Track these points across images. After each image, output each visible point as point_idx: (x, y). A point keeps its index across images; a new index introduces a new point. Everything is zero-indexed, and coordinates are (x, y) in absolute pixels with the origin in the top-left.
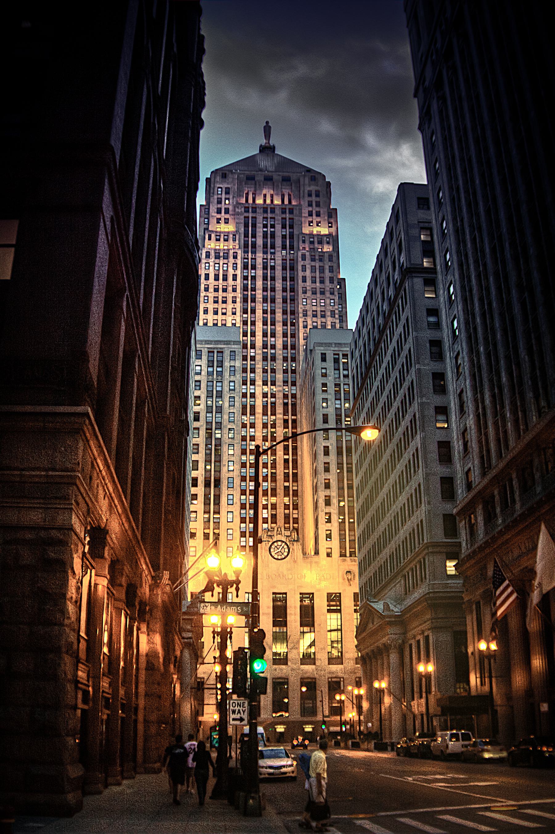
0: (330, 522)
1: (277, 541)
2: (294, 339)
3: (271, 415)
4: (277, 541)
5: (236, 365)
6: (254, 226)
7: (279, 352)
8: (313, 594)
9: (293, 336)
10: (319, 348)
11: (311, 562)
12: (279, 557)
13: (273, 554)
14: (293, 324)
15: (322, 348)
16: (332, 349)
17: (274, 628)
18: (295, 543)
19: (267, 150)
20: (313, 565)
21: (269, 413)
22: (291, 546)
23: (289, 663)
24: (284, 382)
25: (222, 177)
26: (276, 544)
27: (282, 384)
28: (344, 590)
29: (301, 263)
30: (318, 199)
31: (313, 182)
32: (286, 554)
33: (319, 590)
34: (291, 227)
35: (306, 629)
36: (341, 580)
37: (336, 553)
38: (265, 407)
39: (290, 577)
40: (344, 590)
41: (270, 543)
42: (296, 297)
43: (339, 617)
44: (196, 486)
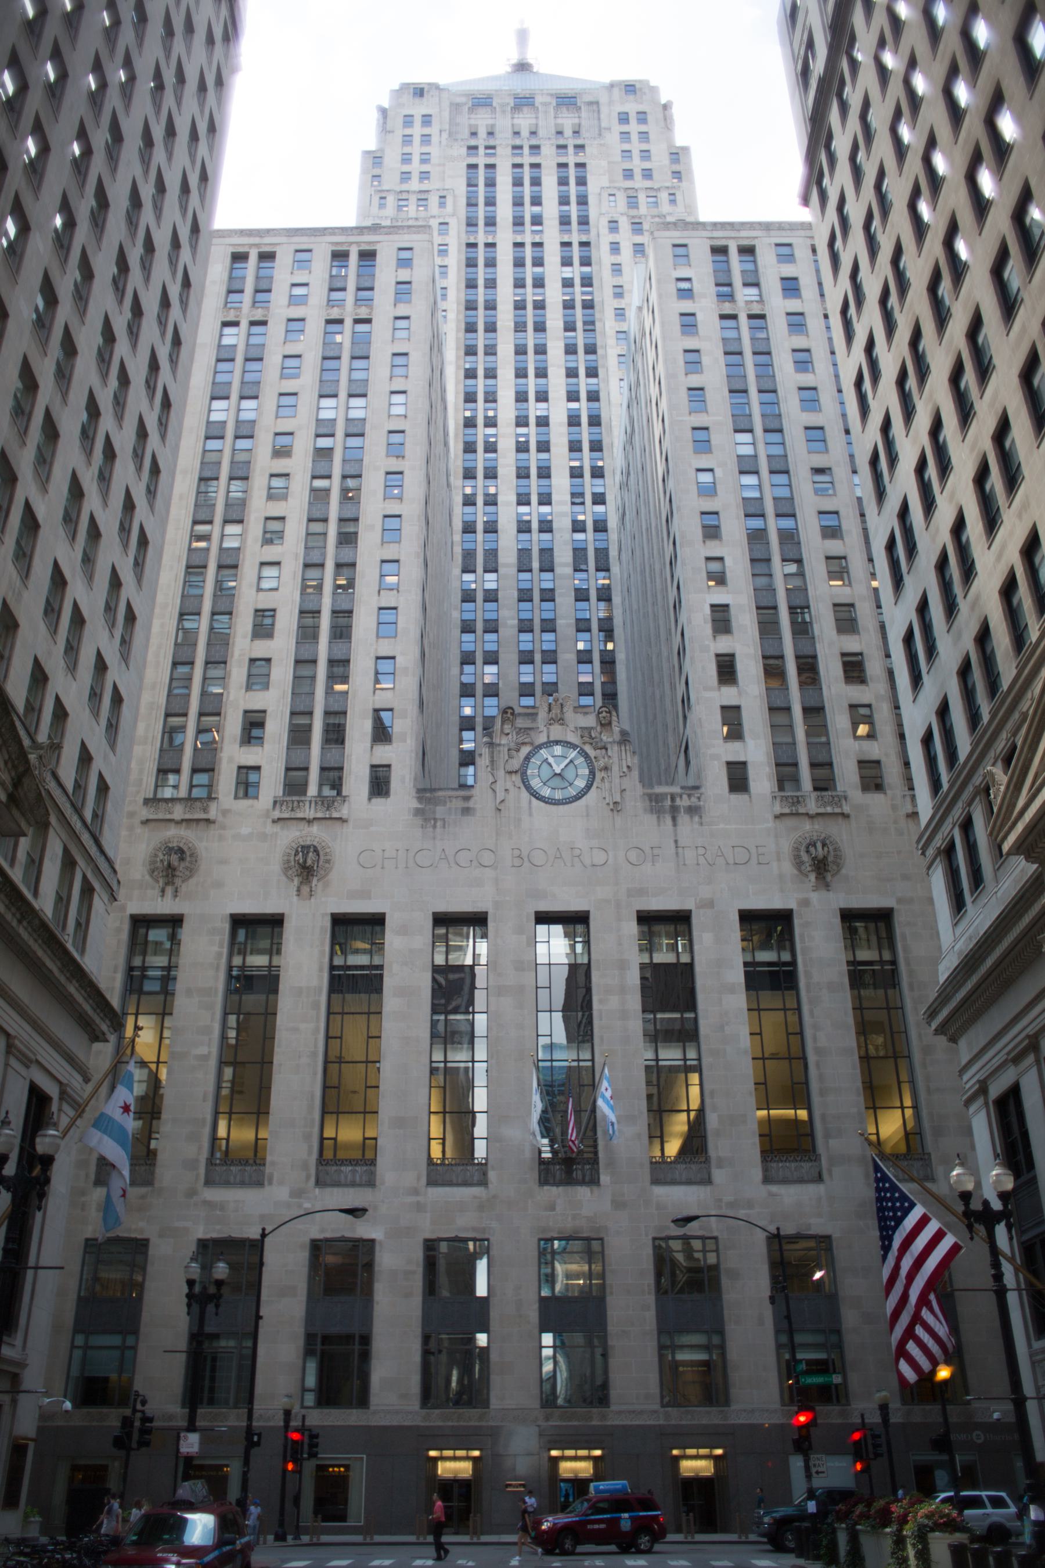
3: (542, 570)
4: (550, 744)
5: (414, 280)
6: (491, 183)
7: (559, 435)
10: (667, 234)
11: (674, 810)
12: (558, 795)
13: (535, 783)
15: (677, 234)
16: (709, 235)
19: (522, 67)
20: (683, 818)
21: (536, 565)
23: (605, 1178)
24: (573, 495)
25: (415, 94)
27: (568, 497)
28: (805, 903)
30: (643, 128)
31: (631, 97)
32: (581, 783)
33: (710, 904)
34: (582, 182)
35: (670, 1055)
36: (788, 867)
38: (524, 554)
39: (599, 857)
40: (805, 903)
41: (525, 750)
42: (597, 316)
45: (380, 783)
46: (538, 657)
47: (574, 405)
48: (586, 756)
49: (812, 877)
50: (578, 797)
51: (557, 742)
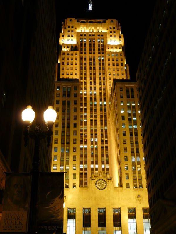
0: (128, 170)
1: (100, 180)
2: (104, 86)
4: (100, 180)
8: (120, 208)
9: (104, 89)
12: (101, 188)
14: (104, 84)
17: (99, 228)
18: (109, 180)
22: (107, 182)
26: (99, 181)
29: (107, 62)
32: (104, 186)
33: (123, 206)
35: (117, 228)
36: (135, 200)
37: (131, 186)
42: (105, 72)
43: (135, 221)
44: (57, 151)
45: (74, 186)
46: (94, 143)
47: (101, 91)
48: (105, 182)
49: (138, 201)
50: (104, 189)
51: (101, 179)
